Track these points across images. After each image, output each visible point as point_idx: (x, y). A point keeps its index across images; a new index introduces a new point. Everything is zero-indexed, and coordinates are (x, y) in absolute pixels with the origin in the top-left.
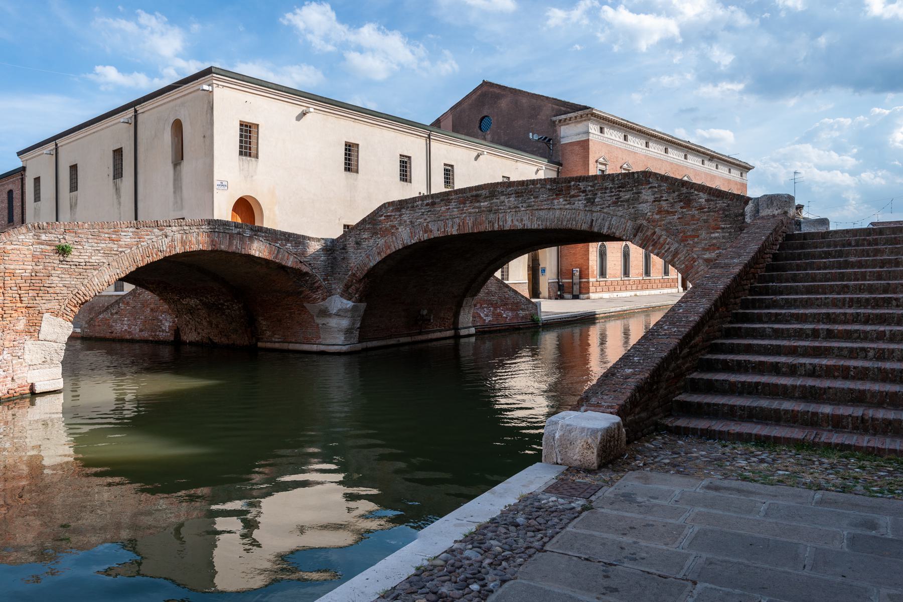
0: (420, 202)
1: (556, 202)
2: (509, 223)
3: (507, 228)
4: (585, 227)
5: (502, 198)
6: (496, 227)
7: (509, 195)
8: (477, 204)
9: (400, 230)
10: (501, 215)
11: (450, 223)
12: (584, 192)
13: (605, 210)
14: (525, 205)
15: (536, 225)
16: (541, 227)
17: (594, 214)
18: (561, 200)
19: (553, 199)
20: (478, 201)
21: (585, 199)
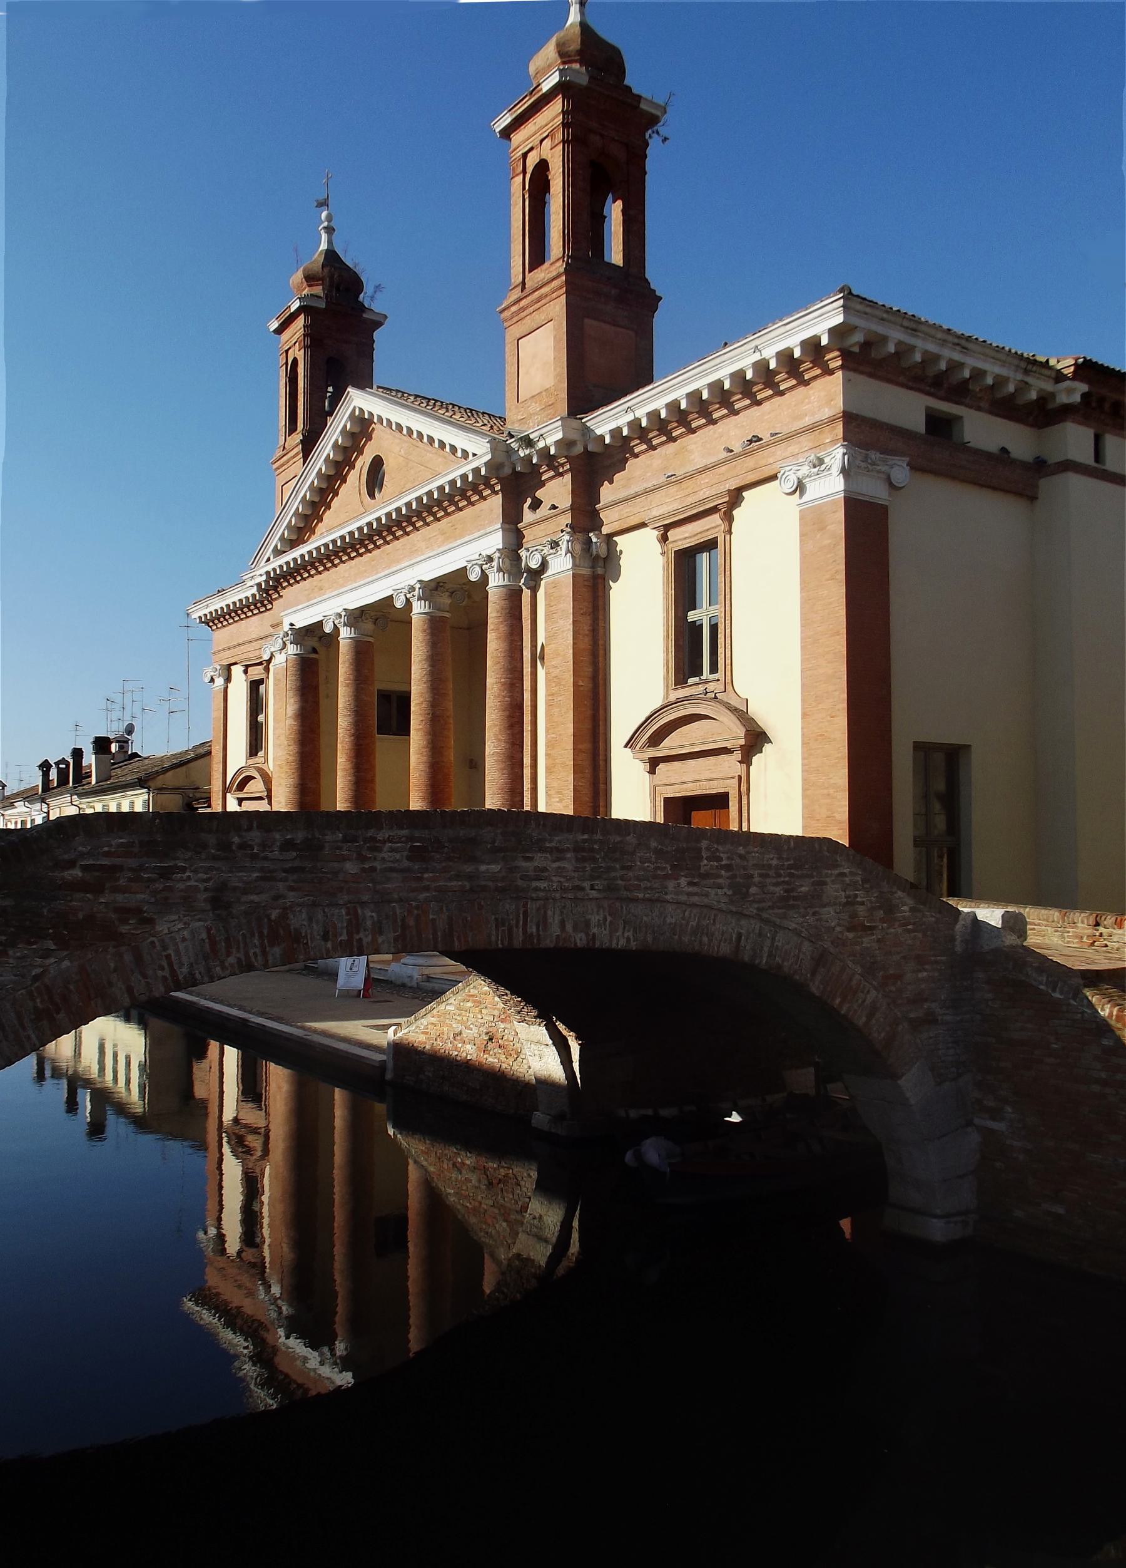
0: (255, 836)
1: (671, 884)
2: (555, 930)
3: (548, 943)
4: (725, 949)
5: (540, 860)
6: (518, 941)
7: (558, 853)
8: (468, 868)
9: (162, 927)
10: (532, 906)
11: (369, 915)
12: (728, 868)
13: (765, 915)
14: (599, 884)
15: (622, 939)
16: (633, 945)
17: (743, 922)
18: (683, 881)
19: (667, 877)
20: (473, 859)
21: (730, 887)
